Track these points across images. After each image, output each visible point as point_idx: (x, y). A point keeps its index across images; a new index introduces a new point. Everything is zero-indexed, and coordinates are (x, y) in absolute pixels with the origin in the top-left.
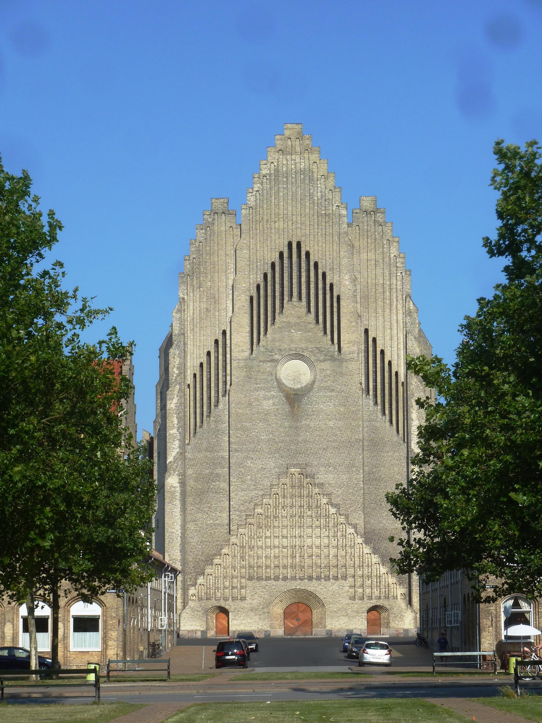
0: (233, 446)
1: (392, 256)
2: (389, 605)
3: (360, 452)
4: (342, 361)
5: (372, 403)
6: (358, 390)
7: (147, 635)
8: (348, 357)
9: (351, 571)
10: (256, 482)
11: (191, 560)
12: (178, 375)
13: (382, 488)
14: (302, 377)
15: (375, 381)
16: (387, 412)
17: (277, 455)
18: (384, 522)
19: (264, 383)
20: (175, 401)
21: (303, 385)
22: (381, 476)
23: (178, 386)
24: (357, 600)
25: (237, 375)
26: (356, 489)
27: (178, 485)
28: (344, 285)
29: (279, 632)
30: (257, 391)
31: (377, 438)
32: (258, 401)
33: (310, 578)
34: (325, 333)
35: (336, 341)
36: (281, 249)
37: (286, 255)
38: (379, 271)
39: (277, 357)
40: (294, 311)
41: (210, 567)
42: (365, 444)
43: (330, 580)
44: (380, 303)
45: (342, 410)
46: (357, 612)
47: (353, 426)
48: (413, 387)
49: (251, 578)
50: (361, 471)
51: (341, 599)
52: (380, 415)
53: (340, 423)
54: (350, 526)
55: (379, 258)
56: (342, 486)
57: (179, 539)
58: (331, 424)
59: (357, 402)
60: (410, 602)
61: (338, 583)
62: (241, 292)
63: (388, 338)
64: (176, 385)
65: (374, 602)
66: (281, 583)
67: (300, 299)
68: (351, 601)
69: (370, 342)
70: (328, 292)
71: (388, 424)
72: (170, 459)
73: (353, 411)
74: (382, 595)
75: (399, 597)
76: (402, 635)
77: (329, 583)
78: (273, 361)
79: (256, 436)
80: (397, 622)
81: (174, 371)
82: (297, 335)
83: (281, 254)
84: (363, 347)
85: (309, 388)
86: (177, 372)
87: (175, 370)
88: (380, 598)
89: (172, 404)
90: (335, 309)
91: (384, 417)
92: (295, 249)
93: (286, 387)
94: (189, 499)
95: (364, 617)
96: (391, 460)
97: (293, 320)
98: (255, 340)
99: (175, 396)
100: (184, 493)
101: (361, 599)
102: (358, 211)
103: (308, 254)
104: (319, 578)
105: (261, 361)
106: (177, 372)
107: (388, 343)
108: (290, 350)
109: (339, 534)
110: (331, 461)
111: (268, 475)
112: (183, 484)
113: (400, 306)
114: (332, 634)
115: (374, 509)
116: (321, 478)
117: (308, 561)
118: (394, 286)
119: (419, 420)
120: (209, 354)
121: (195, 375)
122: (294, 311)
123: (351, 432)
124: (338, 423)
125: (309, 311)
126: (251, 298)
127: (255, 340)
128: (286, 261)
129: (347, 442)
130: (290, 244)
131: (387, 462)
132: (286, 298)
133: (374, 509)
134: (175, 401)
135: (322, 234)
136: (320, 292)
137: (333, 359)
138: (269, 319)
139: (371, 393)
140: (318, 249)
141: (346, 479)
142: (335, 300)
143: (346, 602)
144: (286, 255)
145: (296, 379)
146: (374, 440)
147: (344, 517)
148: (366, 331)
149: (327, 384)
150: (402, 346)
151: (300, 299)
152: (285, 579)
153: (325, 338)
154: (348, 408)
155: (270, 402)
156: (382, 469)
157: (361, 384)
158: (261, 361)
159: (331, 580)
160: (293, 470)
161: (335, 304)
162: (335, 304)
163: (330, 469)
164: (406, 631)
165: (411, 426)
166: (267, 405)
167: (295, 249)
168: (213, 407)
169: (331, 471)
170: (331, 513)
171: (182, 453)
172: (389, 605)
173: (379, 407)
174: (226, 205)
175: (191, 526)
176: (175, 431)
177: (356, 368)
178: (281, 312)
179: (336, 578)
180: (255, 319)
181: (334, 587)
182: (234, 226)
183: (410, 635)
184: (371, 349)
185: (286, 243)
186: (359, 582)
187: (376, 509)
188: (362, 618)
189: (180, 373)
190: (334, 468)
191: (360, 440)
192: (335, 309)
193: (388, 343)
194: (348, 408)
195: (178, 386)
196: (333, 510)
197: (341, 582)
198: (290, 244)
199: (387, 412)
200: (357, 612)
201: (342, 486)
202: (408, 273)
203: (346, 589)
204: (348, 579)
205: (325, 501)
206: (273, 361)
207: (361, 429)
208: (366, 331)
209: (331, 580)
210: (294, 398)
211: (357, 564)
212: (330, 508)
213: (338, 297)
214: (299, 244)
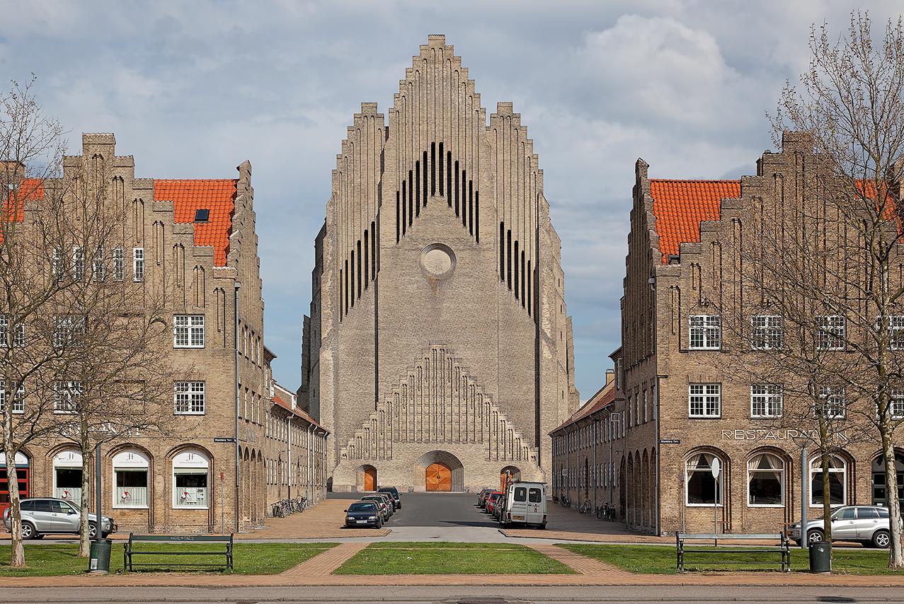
0: (380, 325)
1: (526, 157)
4: (479, 251)
5: (507, 288)
7: (287, 489)
8: (485, 247)
9: (486, 436)
10: (401, 357)
11: (343, 424)
12: (331, 261)
14: (443, 264)
15: (509, 269)
16: (520, 296)
17: (420, 334)
19: (409, 270)
20: (329, 284)
21: (444, 272)
23: (331, 271)
25: (384, 262)
27: (331, 358)
28: (483, 184)
29: (422, 489)
30: (403, 276)
32: (404, 285)
33: (450, 441)
34: (465, 225)
35: (474, 233)
36: (425, 150)
37: (429, 155)
38: (514, 169)
39: (420, 246)
40: (437, 205)
41: (360, 430)
44: (514, 199)
49: (397, 441)
52: (514, 298)
55: (514, 158)
57: (332, 405)
61: (475, 446)
62: (389, 188)
63: (521, 230)
64: (330, 270)
65: (507, 463)
66: (424, 445)
67: (442, 194)
69: (504, 234)
70: (468, 188)
72: (324, 335)
74: (515, 457)
75: (530, 458)
77: (466, 446)
78: (417, 249)
79: (402, 316)
81: (327, 258)
82: (438, 227)
83: (425, 154)
84: (499, 239)
85: (449, 275)
86: (330, 258)
87: (329, 256)
89: (327, 285)
90: (474, 204)
92: (437, 150)
93: (429, 273)
94: (342, 371)
97: (436, 213)
98: (401, 231)
99: (329, 280)
100: (336, 365)
102: (496, 116)
103: (449, 154)
104: (458, 441)
105: (406, 250)
106: (330, 258)
107: (521, 235)
108: (433, 240)
109: (476, 403)
111: (412, 351)
112: (336, 358)
113: (533, 203)
115: (508, 382)
116: (459, 354)
117: (448, 427)
118: (527, 184)
119: (549, 304)
120: (359, 243)
121: (347, 261)
122: (437, 205)
125: (450, 205)
126: (398, 193)
127: (401, 231)
128: (429, 160)
130: (433, 145)
132: (429, 193)
133: (508, 382)
134: (329, 284)
135: (462, 136)
136: (461, 188)
137: (472, 249)
138: (414, 212)
139: (506, 279)
140: (459, 150)
142: (474, 195)
144: (429, 155)
145: (438, 267)
148: (502, 224)
150: (534, 238)
151: (442, 194)
152: (428, 441)
153: (464, 230)
155: (415, 286)
158: (406, 250)
160: (434, 346)
161: (474, 200)
162: (474, 200)
166: (412, 288)
167: (437, 150)
168: (362, 290)
170: (469, 384)
171: (335, 331)
173: (513, 292)
174: (374, 109)
175: (343, 395)
176: (328, 311)
177: (494, 255)
178: (425, 205)
179: (473, 441)
180: (401, 212)
182: (382, 128)
184: (506, 240)
185: (430, 144)
186: (494, 446)
189: (333, 260)
192: (474, 204)
193: (521, 235)
195: (331, 271)
196: (470, 382)
198: (433, 145)
199: (520, 296)
202: (540, 172)
205: (463, 374)
206: (417, 249)
208: (502, 224)
210: (437, 283)
211: (492, 429)
212: (468, 380)
213: (477, 193)
214: (441, 145)
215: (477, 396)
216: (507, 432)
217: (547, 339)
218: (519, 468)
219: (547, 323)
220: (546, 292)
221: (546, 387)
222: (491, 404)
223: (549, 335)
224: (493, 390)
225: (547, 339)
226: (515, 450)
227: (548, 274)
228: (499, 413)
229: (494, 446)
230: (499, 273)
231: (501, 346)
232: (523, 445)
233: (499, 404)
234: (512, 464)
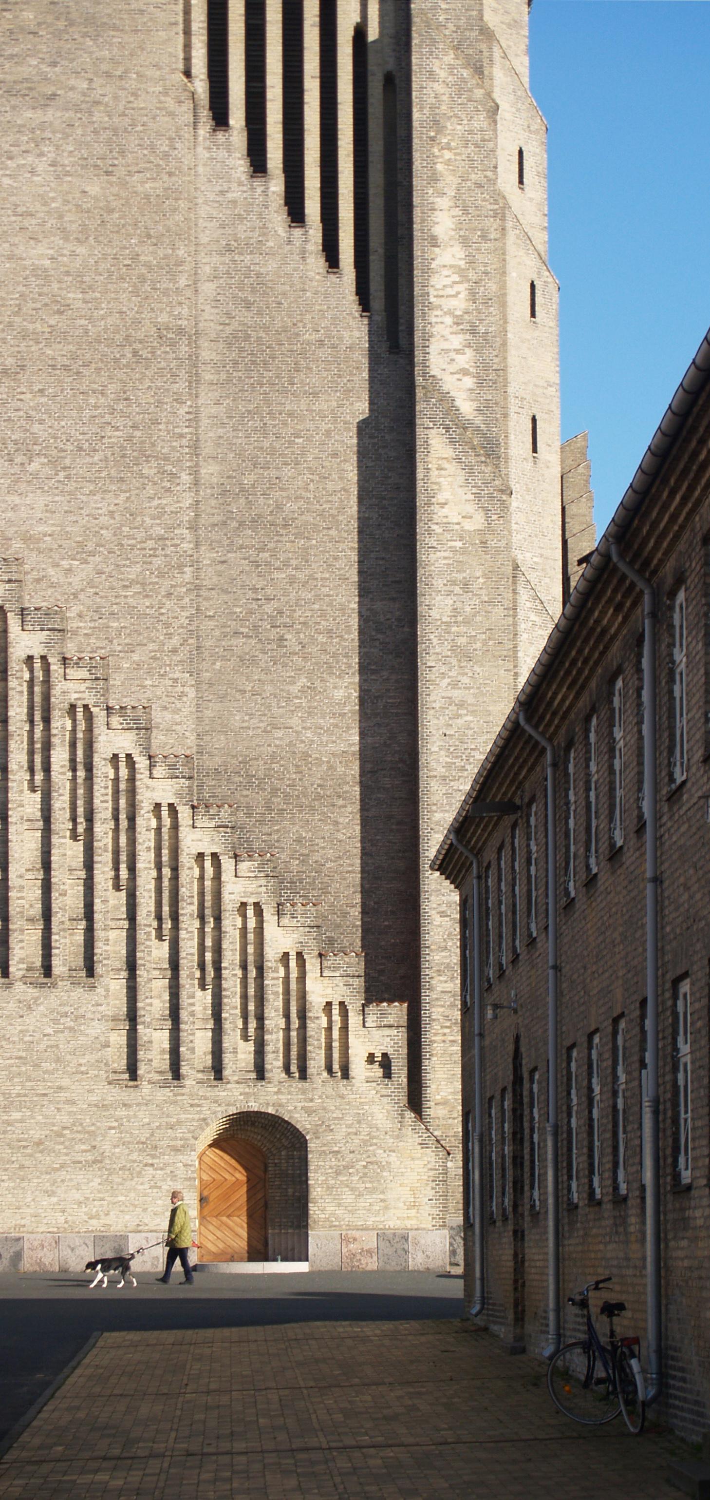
2: (309, 1112)
3: (181, 386)
5: (240, 164)
6: (170, 103)
13: (286, 564)
16: (313, 206)
18: (295, 721)
22: (279, 507)
24: (146, 1088)
26: (158, 562)
31: (266, 328)
42: (207, 353)
43: (9, 986)
45: (94, 189)
46: (149, 1147)
47: (148, 266)
48: (439, 88)
50: (185, 478)
51: (66, 1082)
52: (278, 217)
53: (81, 250)
54: (115, 720)
56: (90, 546)
58: (39, 254)
59: (166, 155)
60: (415, 1099)
68: (116, 1094)
71: (317, 263)
73: (147, 197)
76: (371, 1264)
80: (348, 1197)
88: (260, 1072)
91: (297, 232)
95: (181, 1172)
96: (328, 433)
101: (165, 1085)
110: (36, 428)
114: (18, 1256)
115: (246, 661)
119: (465, 242)
123: (136, 293)
124: (73, 254)
129: (119, 338)
131: (309, 439)
133: (246, 661)
141: (111, 514)
143: (93, 1098)
146: (247, 337)
147: (84, 673)
149: (25, 71)
154: (123, 184)
156: (288, 472)
157: (188, 73)
159: (19, 987)
163: (34, 467)
164: (398, 1241)
165: (428, 271)
169: (36, 475)
172: (309, 1112)
173: (277, 185)
181: (31, 1021)
183: (416, 1261)
187: (254, 660)
188: (173, 1176)
190: (53, 463)
191: (181, 331)
194: (123, 184)
197: (66, 995)
199: (313, 206)
200: (149, 1147)
201: (90, 546)
203: (93, 1032)
204: (105, 980)
207: (183, 281)
209: (19, 987)
215: (61, 723)
216: (231, 924)
217: (455, 426)
218: (301, 1121)
219: (457, 341)
220: (450, 182)
221: (455, 685)
222: (141, 763)
223: (466, 407)
224: (177, 727)
225: (455, 426)
226: (274, 1020)
227: (460, 88)
228: (184, 813)
229: (154, 1001)
230: (201, 85)
231: (209, 471)
232: (321, 989)
233: (185, 767)
234: (278, 1097)
